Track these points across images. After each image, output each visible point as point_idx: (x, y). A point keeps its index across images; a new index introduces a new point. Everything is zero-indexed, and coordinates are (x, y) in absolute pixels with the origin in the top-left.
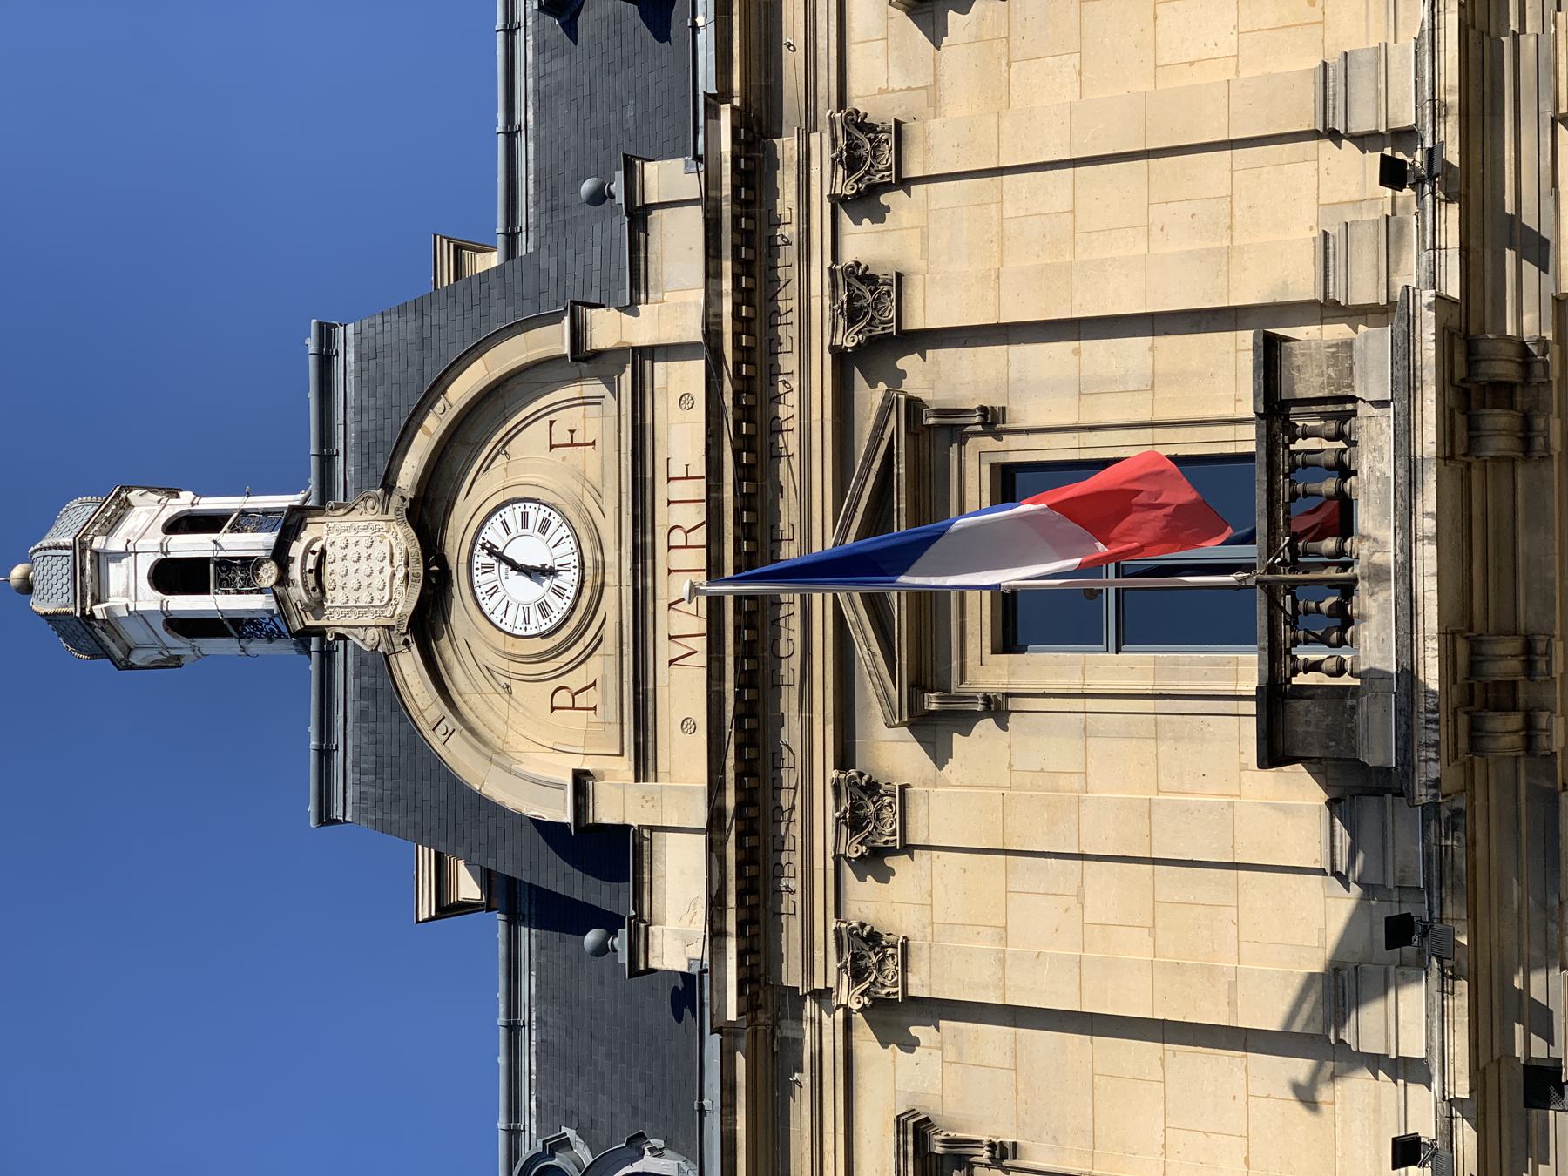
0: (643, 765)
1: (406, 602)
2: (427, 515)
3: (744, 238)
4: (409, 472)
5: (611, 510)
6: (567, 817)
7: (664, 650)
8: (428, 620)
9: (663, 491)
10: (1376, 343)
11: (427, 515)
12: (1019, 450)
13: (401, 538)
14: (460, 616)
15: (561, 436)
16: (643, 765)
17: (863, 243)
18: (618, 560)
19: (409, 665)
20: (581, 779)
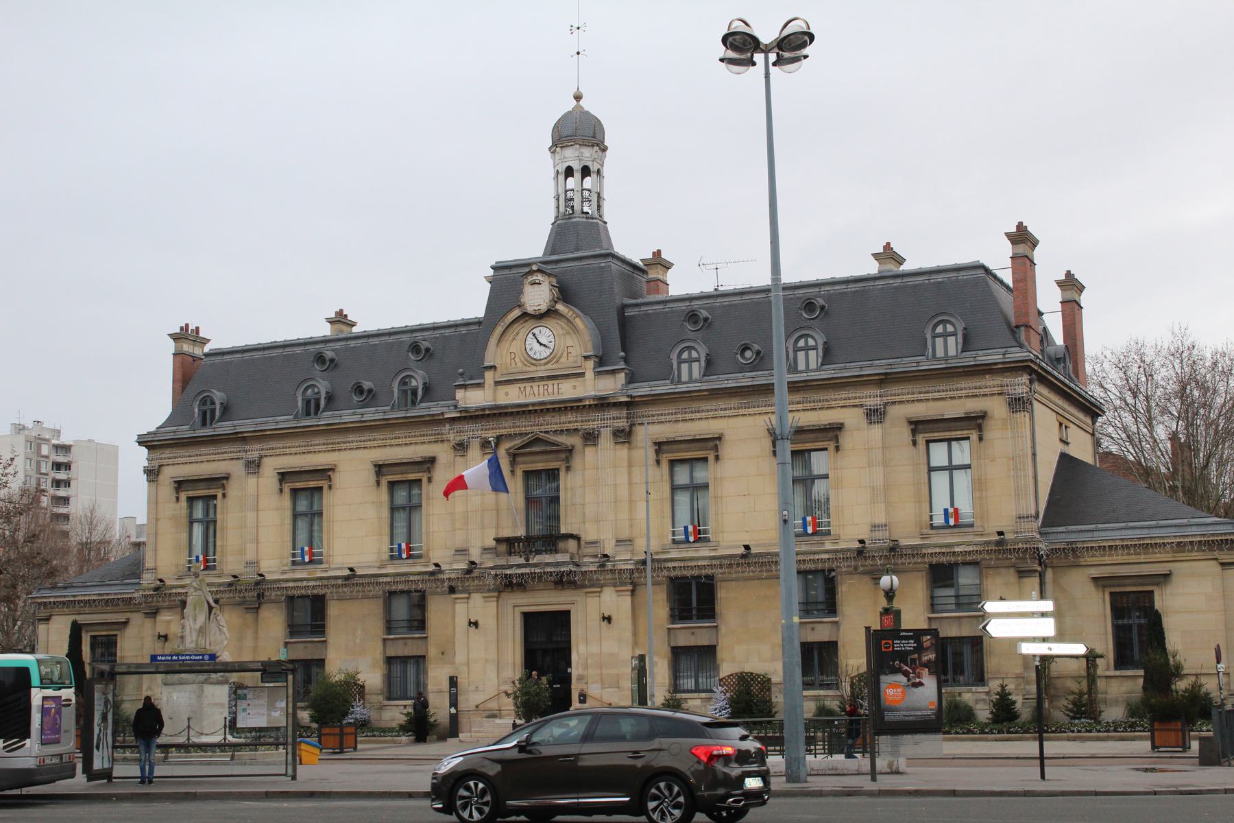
0: (498, 383)
1: (530, 310)
2: (550, 313)
3: (602, 405)
4: (560, 307)
5: (555, 366)
6: (486, 364)
7: (522, 385)
8: (525, 316)
9: (555, 382)
10: (566, 558)
11: (550, 313)
12: (562, 474)
13: (544, 308)
14: (531, 323)
15: (570, 350)
16: (498, 383)
17: (606, 434)
18: (541, 372)
19: (517, 313)
20: (493, 367)
